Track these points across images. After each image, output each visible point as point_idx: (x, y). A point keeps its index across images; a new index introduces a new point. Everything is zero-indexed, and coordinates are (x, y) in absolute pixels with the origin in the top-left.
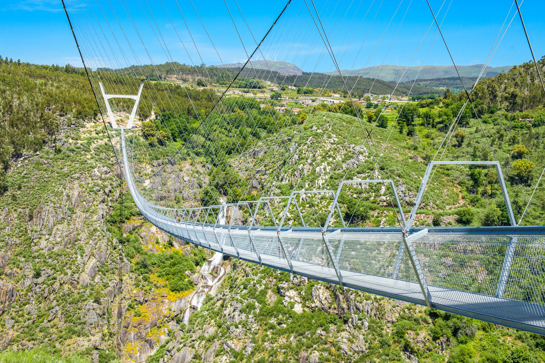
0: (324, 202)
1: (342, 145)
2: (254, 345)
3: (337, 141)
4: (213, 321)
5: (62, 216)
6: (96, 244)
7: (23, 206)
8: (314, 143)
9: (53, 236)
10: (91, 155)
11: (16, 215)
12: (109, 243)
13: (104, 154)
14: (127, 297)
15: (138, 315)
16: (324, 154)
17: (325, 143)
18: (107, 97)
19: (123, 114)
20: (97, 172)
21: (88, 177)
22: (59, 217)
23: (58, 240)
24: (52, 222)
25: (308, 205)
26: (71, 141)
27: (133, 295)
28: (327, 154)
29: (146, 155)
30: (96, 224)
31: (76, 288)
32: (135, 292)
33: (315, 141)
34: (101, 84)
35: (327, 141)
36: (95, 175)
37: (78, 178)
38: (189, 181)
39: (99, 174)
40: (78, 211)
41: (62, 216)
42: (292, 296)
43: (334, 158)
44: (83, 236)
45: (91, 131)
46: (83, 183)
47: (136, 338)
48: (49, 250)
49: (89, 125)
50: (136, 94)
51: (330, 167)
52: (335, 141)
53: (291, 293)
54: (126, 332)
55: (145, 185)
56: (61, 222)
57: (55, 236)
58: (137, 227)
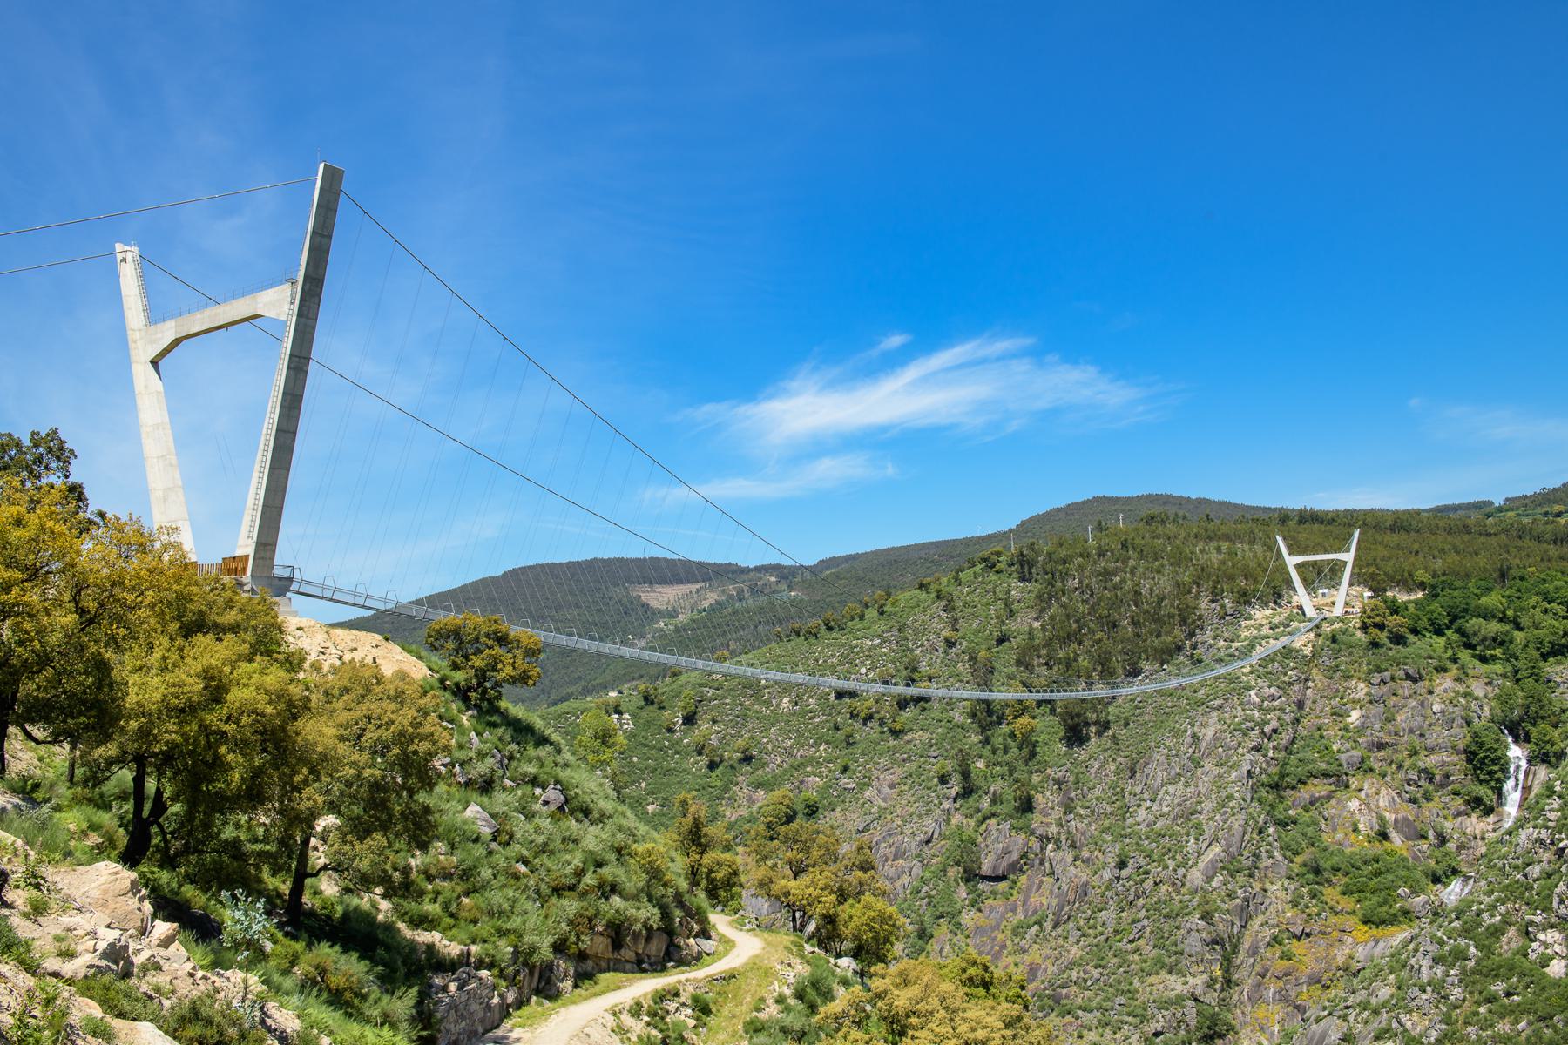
2: (1444, 1027)
4: (1392, 977)
5: (1178, 770)
6: (1225, 821)
7: (1126, 753)
9: (1157, 802)
11: (1113, 768)
13: (1276, 664)
14: (1271, 922)
15: (1287, 956)
18: (1291, 561)
22: (1173, 772)
23: (1165, 810)
24: (1159, 780)
26: (1221, 643)
27: (1284, 921)
29: (1360, 664)
31: (1179, 893)
32: (1289, 914)
34: (1357, 534)
36: (1249, 702)
37: (1220, 708)
38: (1443, 712)
39: (1257, 700)
40: (1207, 764)
41: (1178, 770)
42: (1550, 941)
44: (1207, 806)
45: (1262, 625)
47: (1277, 997)
48: (1148, 826)
49: (1260, 615)
50: (1348, 550)
53: (1550, 935)
54: (1259, 985)
56: (1173, 780)
57: (1160, 804)
58: (1319, 798)
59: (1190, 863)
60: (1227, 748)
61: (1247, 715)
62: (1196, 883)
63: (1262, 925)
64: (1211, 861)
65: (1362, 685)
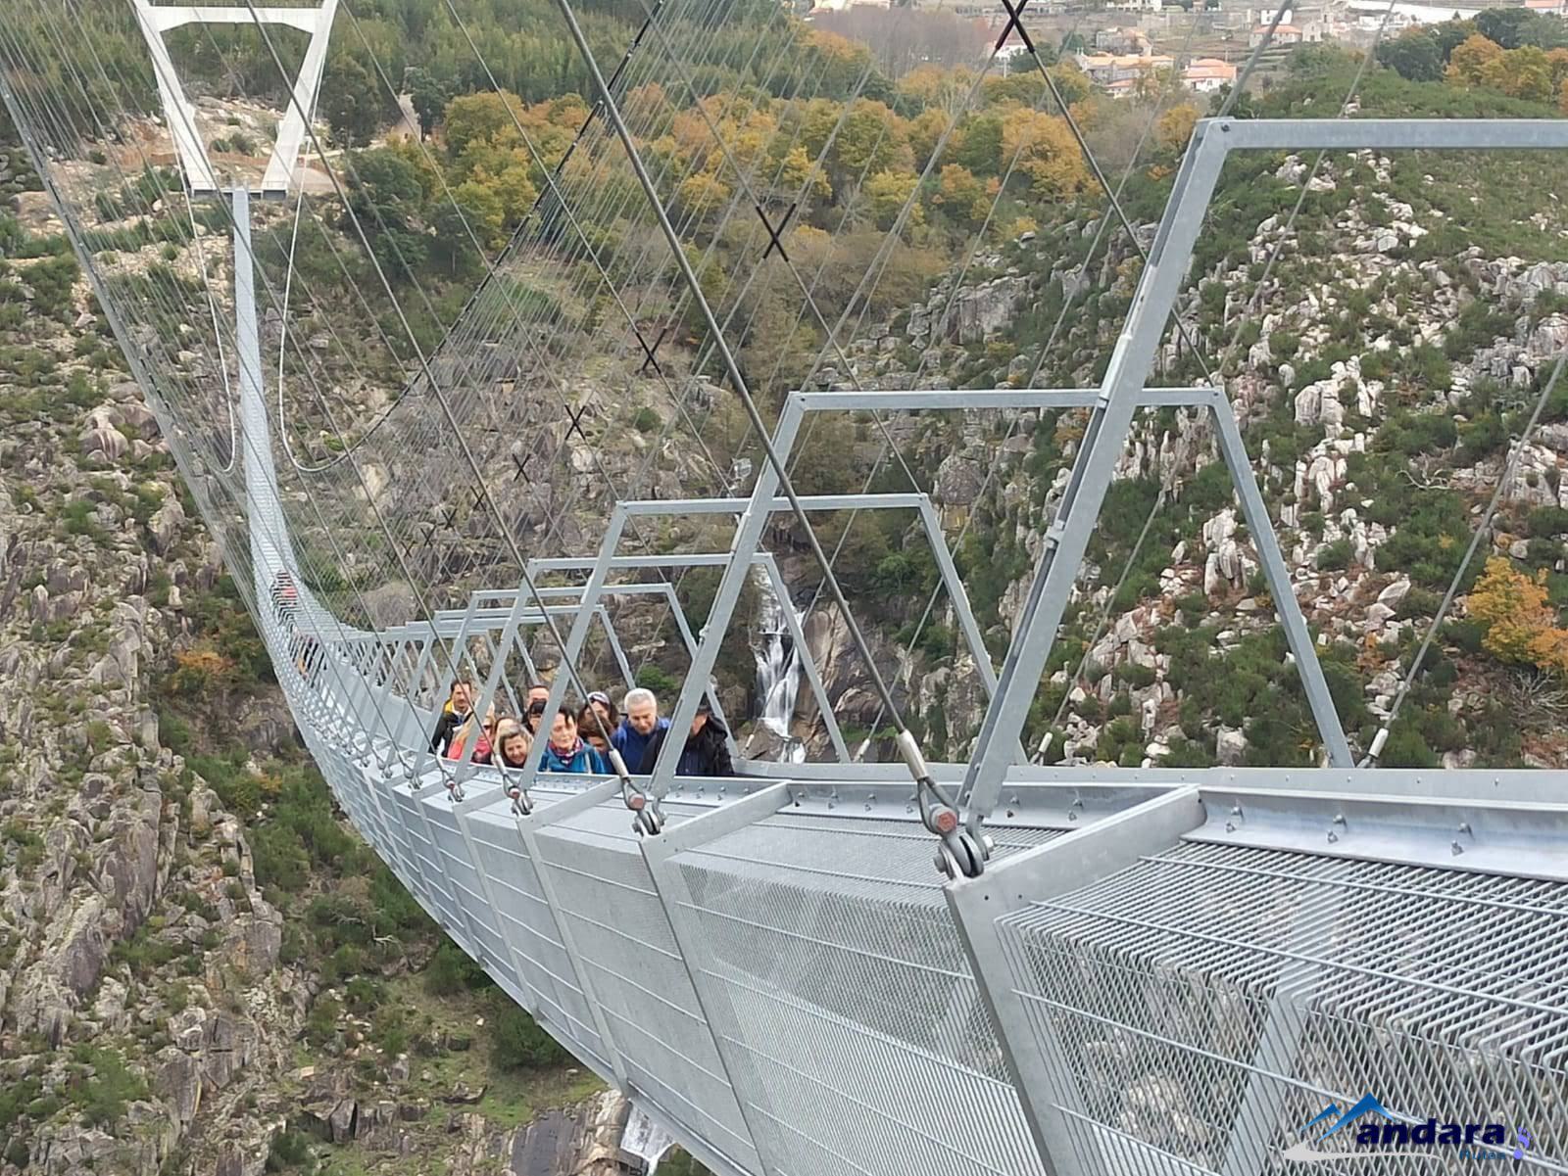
0: (1343, 582)
1: (1445, 262)
3: (1420, 239)
6: (102, 813)
8: (1291, 251)
10: (76, 333)
12: (173, 809)
14: (262, 1099)
16: (1344, 313)
17: (1355, 251)
18: (158, 21)
19: (248, 114)
20: (104, 424)
21: (58, 456)
25: (1249, 604)
28: (1365, 313)
30: (103, 707)
32: (308, 1071)
33: (1294, 242)
35: (1360, 242)
36: (96, 443)
38: (597, 470)
39: (117, 436)
43: (1401, 337)
45: (79, 209)
46: (33, 486)
49: (69, 174)
51: (1376, 387)
52: (1405, 238)
55: (361, 494)
59: (21, 952)
60: (59, 586)
61: (97, 485)
62: (52, 1012)
63: (237, 1114)
64: (82, 940)
65: (380, 395)
